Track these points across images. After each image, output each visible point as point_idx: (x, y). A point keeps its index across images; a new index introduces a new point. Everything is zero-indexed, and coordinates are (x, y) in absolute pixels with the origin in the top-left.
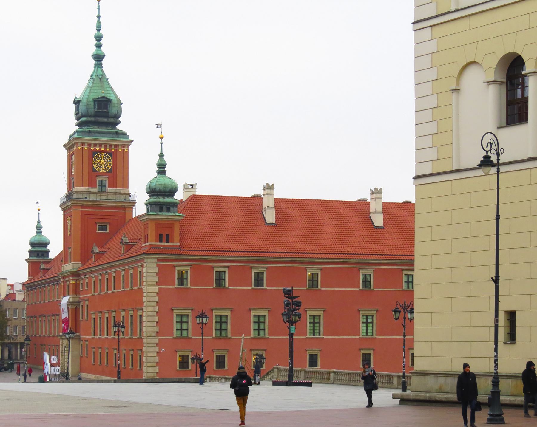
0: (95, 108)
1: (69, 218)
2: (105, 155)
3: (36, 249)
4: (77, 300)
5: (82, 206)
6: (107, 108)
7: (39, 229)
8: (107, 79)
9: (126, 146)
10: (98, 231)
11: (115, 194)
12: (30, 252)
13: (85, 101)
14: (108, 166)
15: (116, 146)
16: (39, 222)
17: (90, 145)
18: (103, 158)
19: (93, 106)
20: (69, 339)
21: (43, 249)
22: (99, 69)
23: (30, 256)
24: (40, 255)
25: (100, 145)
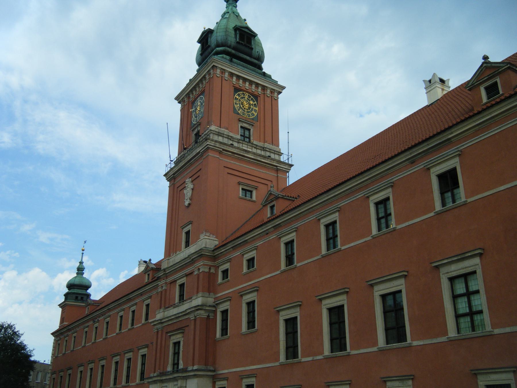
0: (236, 37)
1: (188, 181)
2: (250, 97)
3: (75, 291)
4: (210, 301)
5: (220, 152)
6: (250, 43)
7: (80, 270)
8: (245, 20)
9: (276, 94)
10: (241, 196)
11: (264, 149)
12: (66, 295)
13: (223, 27)
14: (253, 112)
15: (264, 88)
16: (81, 263)
17: (232, 75)
18: (246, 99)
19: (233, 36)
20: (186, 378)
21: (83, 292)
22: (234, 8)
23: (66, 299)
24: (79, 298)
25: (245, 80)
